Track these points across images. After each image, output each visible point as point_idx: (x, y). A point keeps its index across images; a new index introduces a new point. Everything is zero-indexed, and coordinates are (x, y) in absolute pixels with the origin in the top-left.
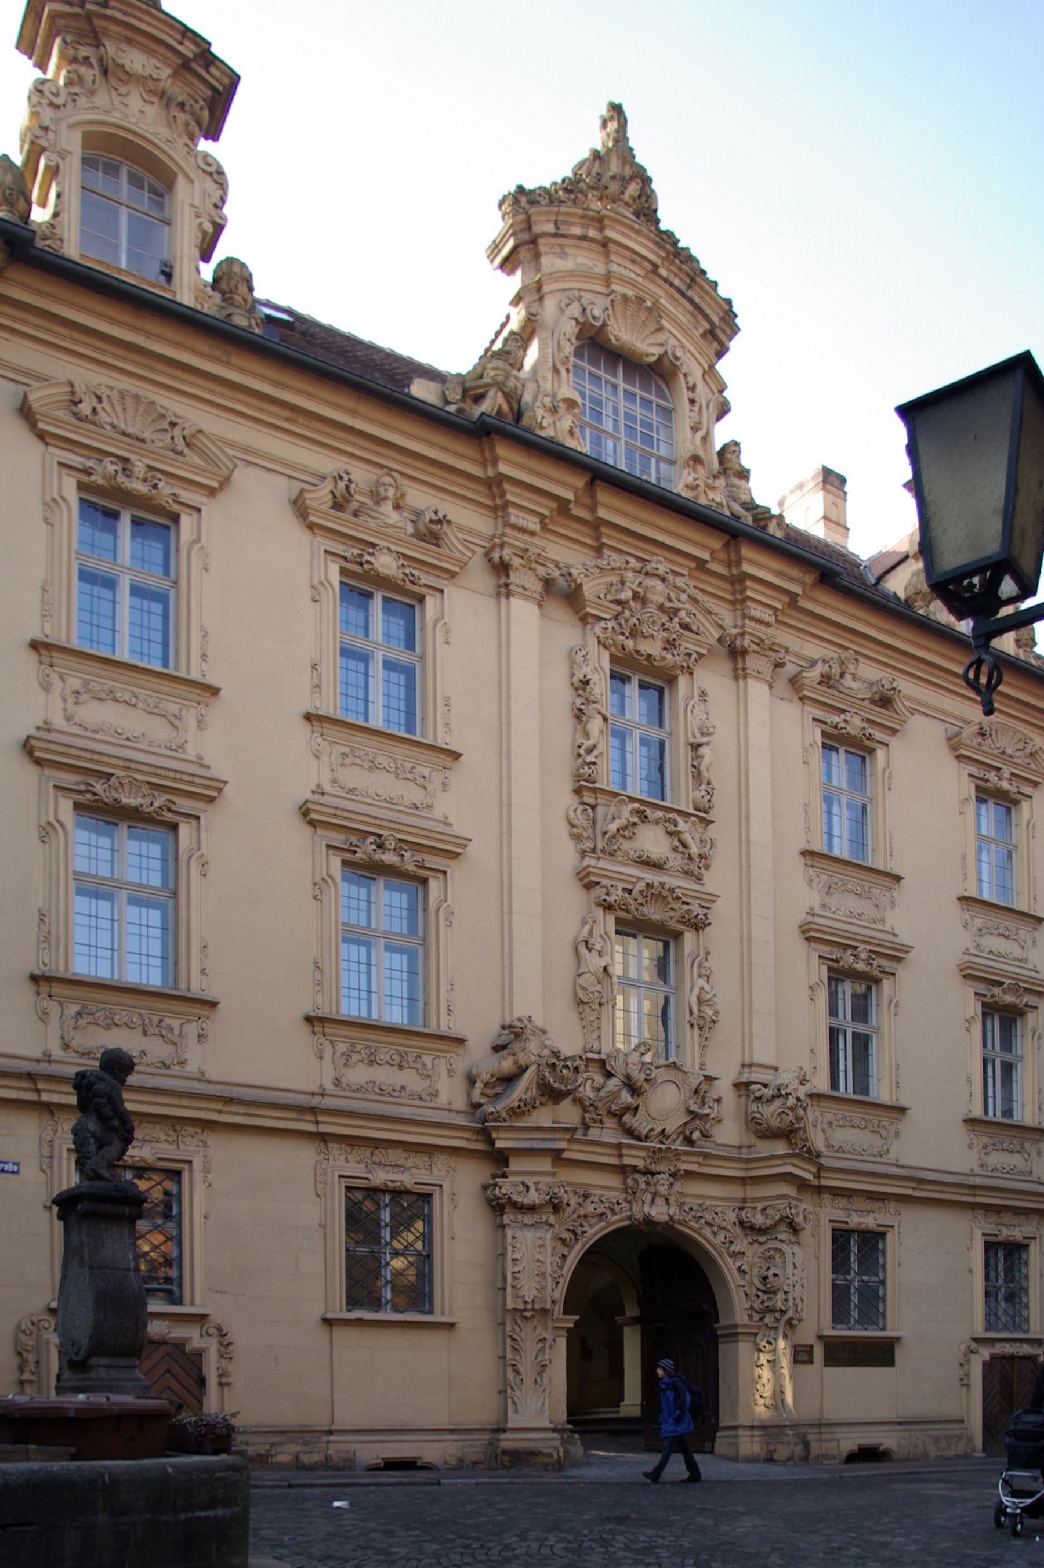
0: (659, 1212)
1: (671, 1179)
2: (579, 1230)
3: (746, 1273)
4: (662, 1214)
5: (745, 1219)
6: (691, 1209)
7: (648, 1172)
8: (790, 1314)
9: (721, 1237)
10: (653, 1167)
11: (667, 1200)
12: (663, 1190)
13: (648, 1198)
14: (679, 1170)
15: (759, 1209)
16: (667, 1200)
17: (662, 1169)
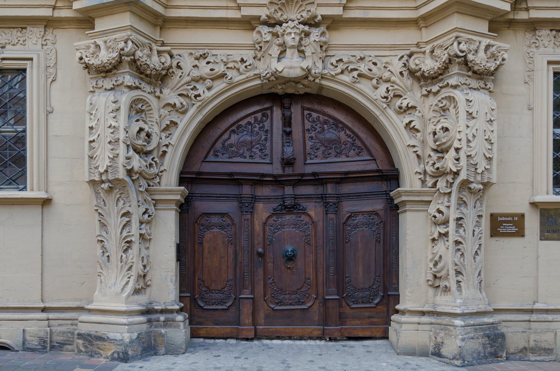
0: (291, 66)
1: (306, 28)
2: (192, 93)
3: (415, 130)
4: (291, 68)
5: (413, 66)
6: (341, 60)
7: (271, 23)
8: (463, 176)
9: (383, 88)
10: (278, 16)
11: (302, 52)
12: (289, 40)
13: (275, 51)
14: (316, 17)
15: (428, 51)
16: (302, 52)
17: (293, 17)
